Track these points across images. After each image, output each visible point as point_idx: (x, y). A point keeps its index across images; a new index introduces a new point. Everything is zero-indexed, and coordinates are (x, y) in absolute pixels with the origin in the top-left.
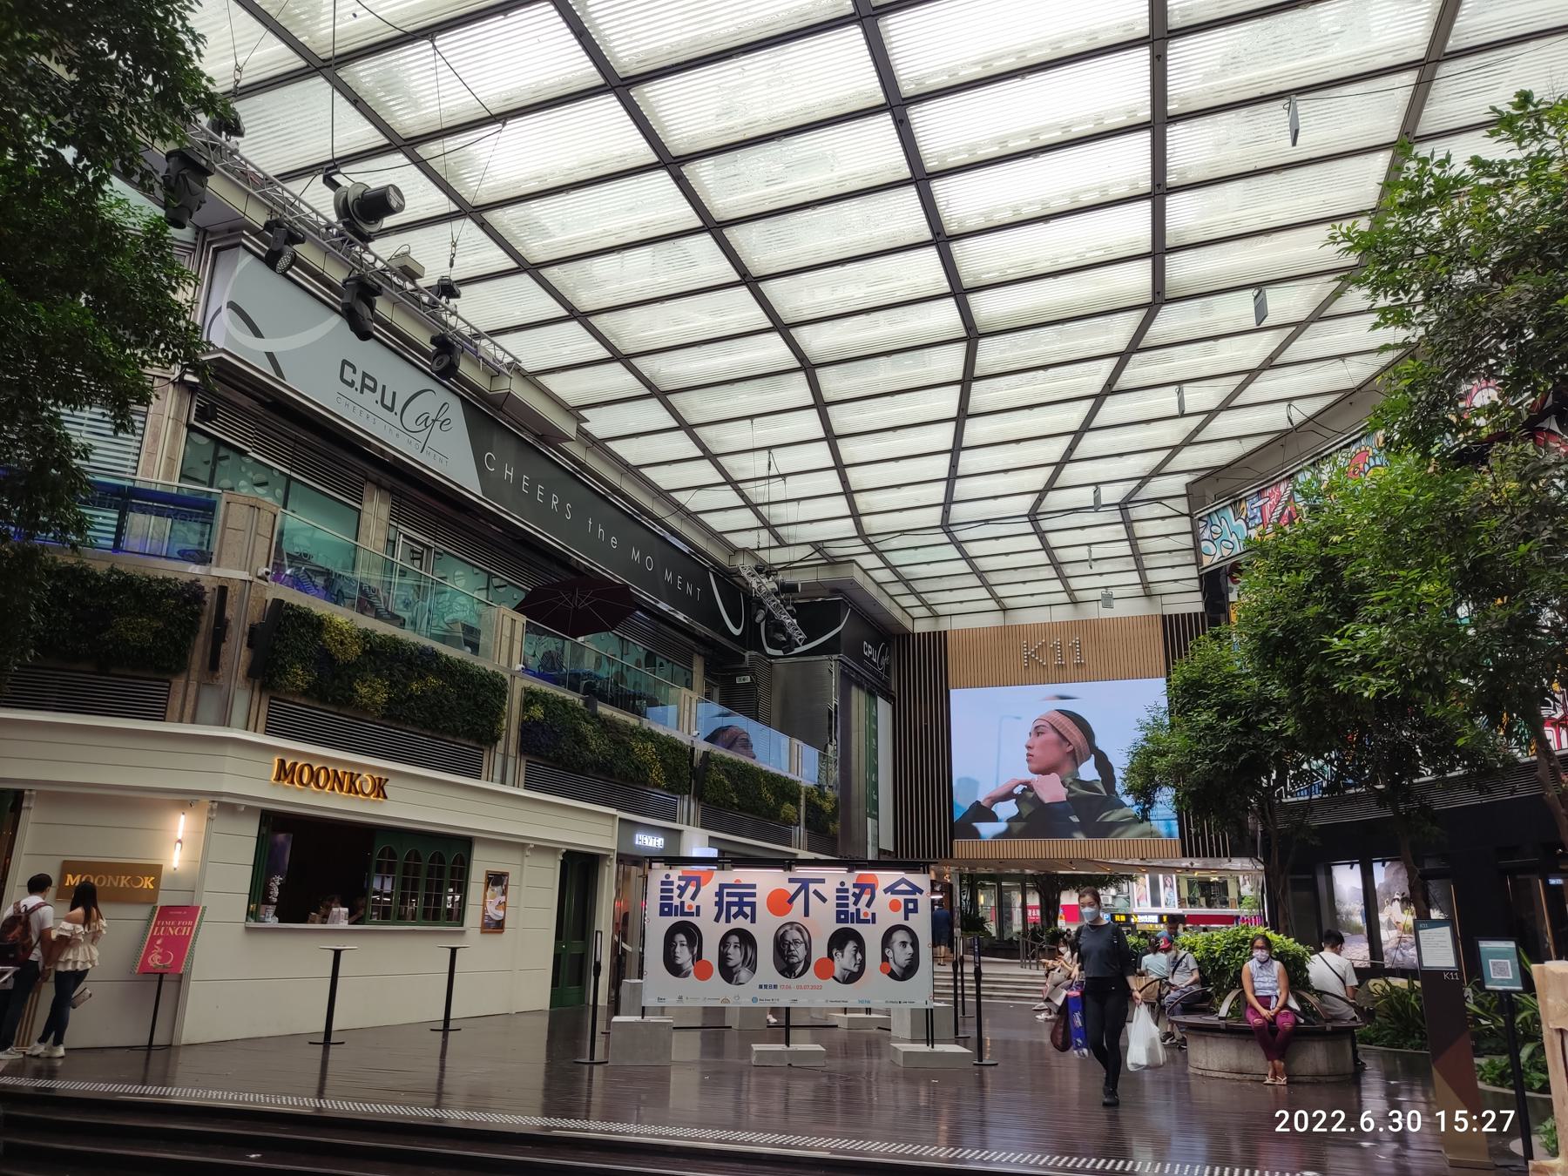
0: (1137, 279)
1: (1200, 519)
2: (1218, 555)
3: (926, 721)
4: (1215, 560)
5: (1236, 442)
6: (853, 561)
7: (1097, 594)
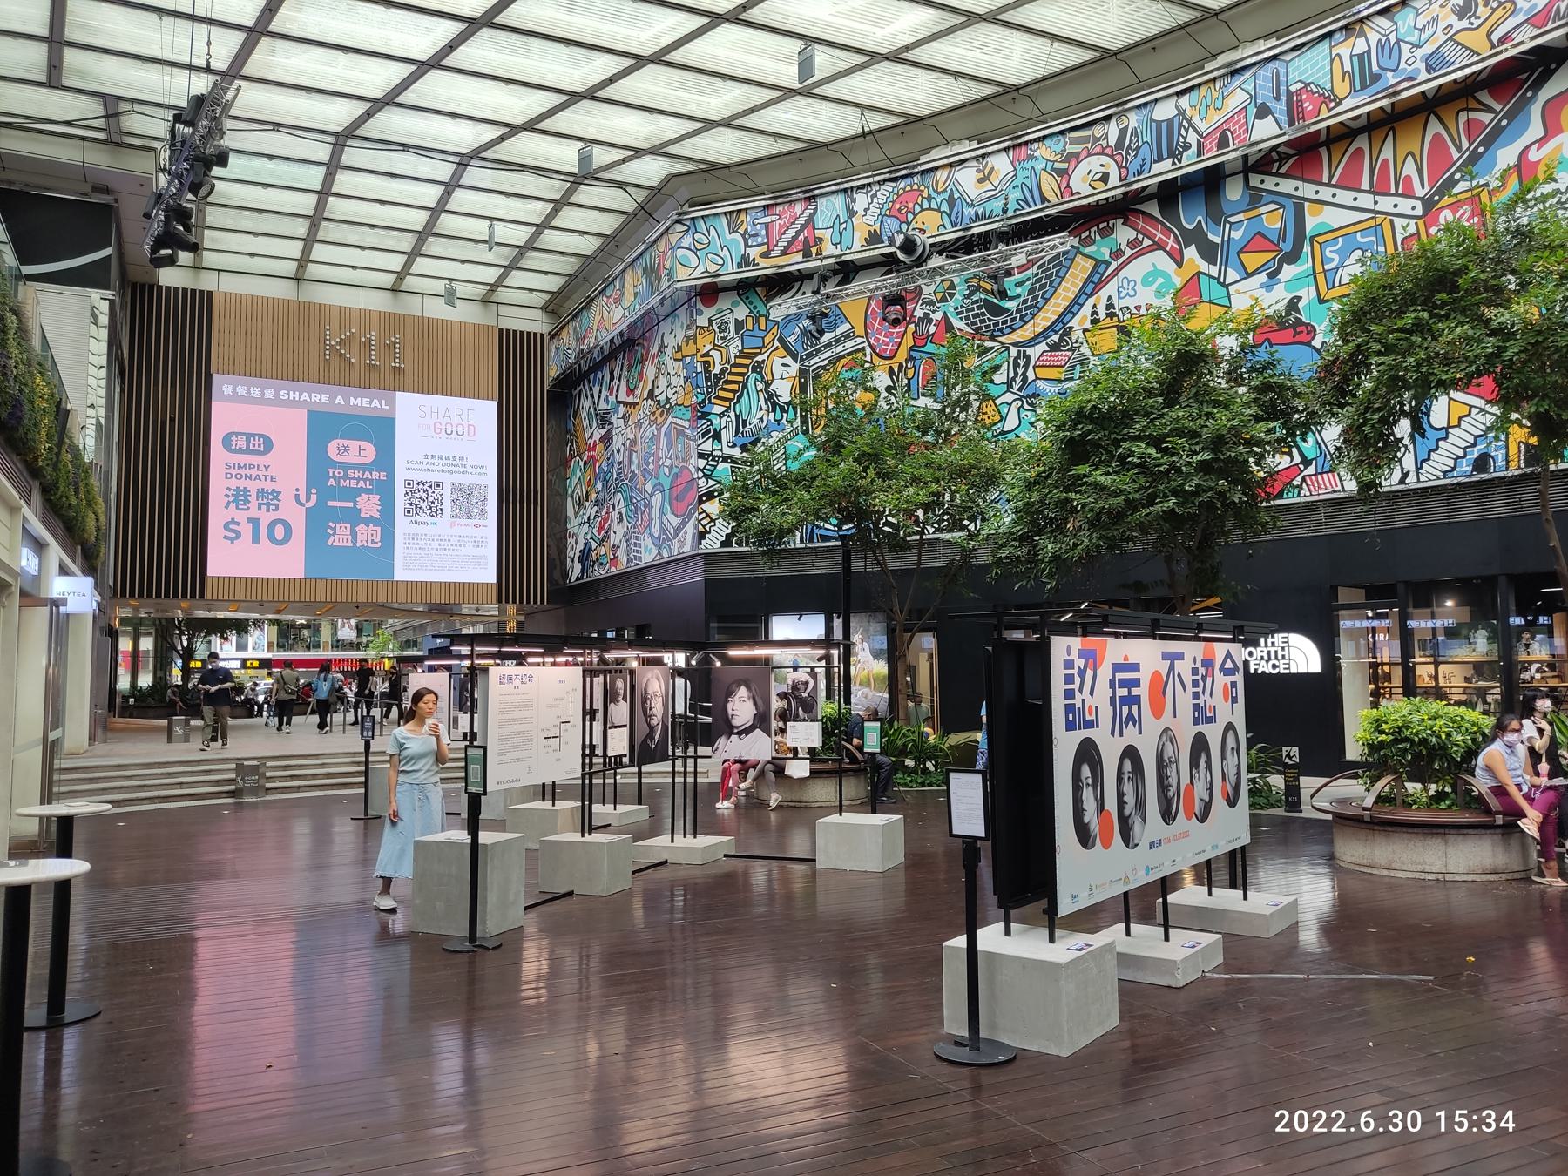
2: (701, 269)
3: (173, 411)
4: (696, 275)
6: (153, 150)
7: (439, 287)
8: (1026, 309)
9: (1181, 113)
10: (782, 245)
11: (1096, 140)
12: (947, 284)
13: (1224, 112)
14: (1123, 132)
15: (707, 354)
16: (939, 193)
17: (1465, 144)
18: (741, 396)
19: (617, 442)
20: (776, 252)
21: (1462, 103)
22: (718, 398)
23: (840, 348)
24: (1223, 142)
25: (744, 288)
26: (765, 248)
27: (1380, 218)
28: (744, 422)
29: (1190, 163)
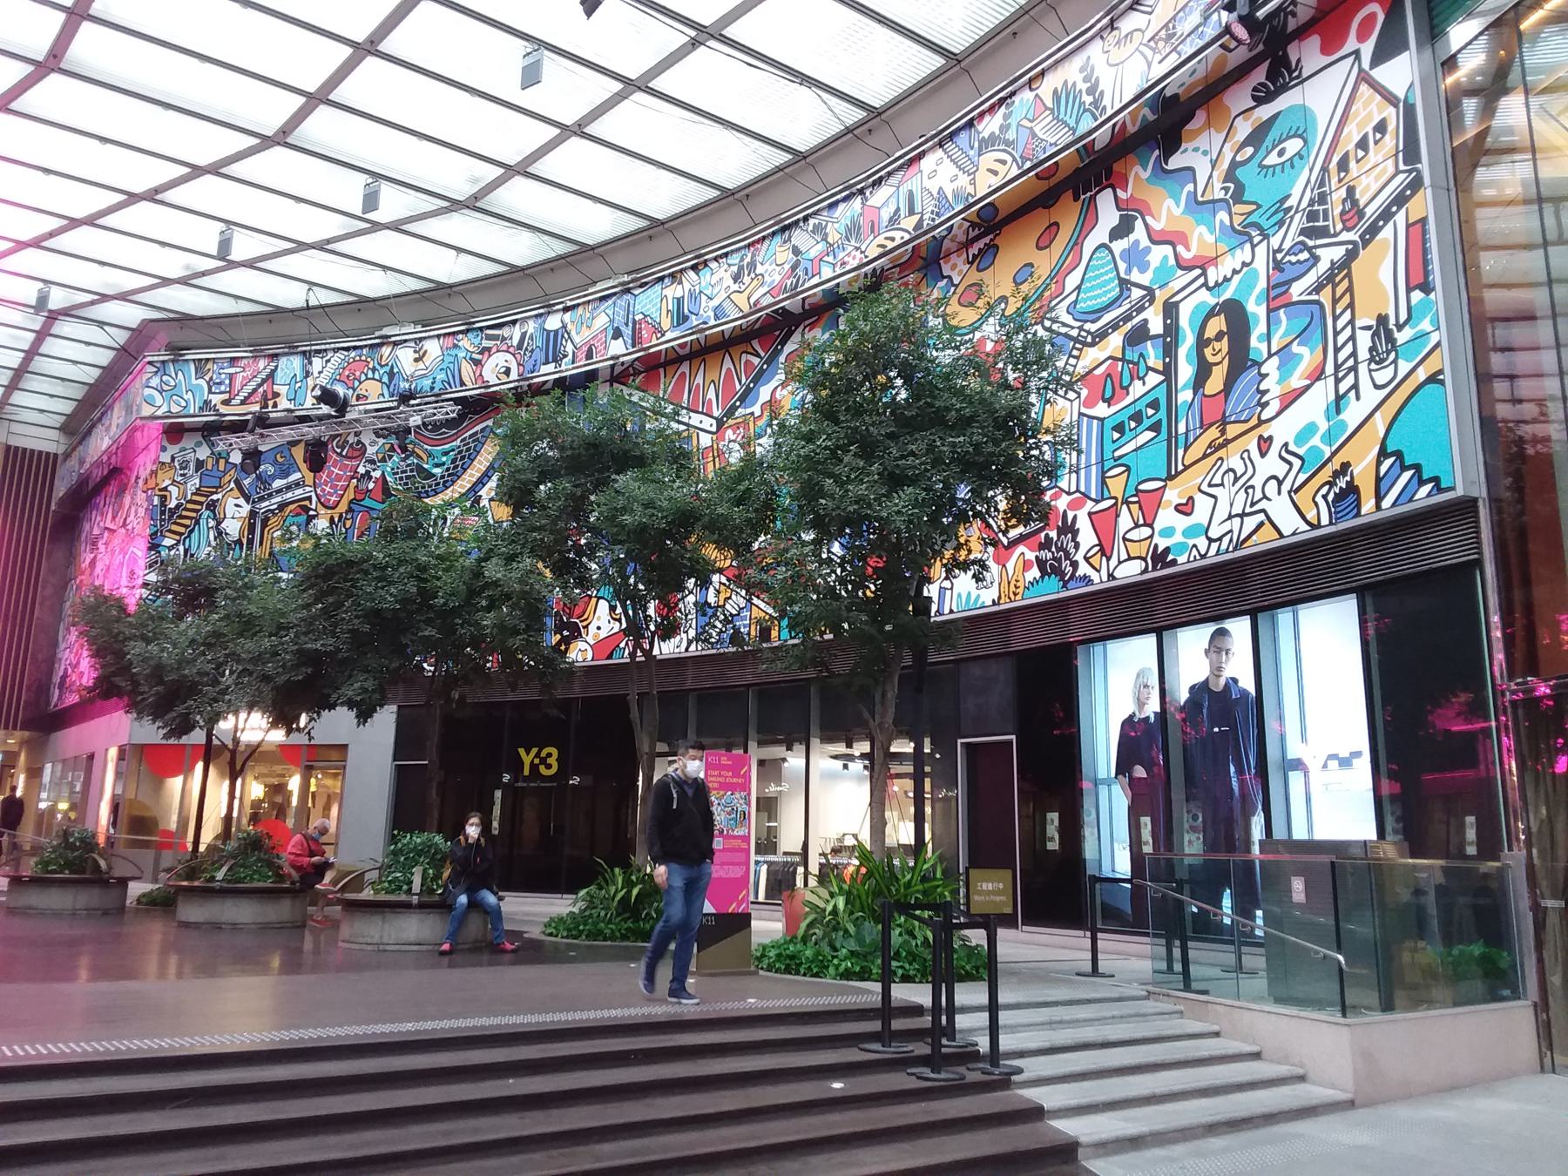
0: (274, 110)
1: (150, 363)
2: (165, 408)
4: (159, 413)
5: (232, 300)
8: (449, 475)
9: (564, 327)
10: (243, 394)
11: (504, 339)
12: (387, 447)
13: (593, 329)
14: (523, 335)
15: (165, 489)
16: (382, 366)
17: (743, 381)
18: (192, 531)
19: (100, 566)
20: (237, 401)
21: (743, 347)
22: (170, 531)
23: (290, 495)
24: (589, 355)
25: (210, 430)
26: (226, 396)
27: (692, 430)
28: (192, 555)
29: (567, 369)
